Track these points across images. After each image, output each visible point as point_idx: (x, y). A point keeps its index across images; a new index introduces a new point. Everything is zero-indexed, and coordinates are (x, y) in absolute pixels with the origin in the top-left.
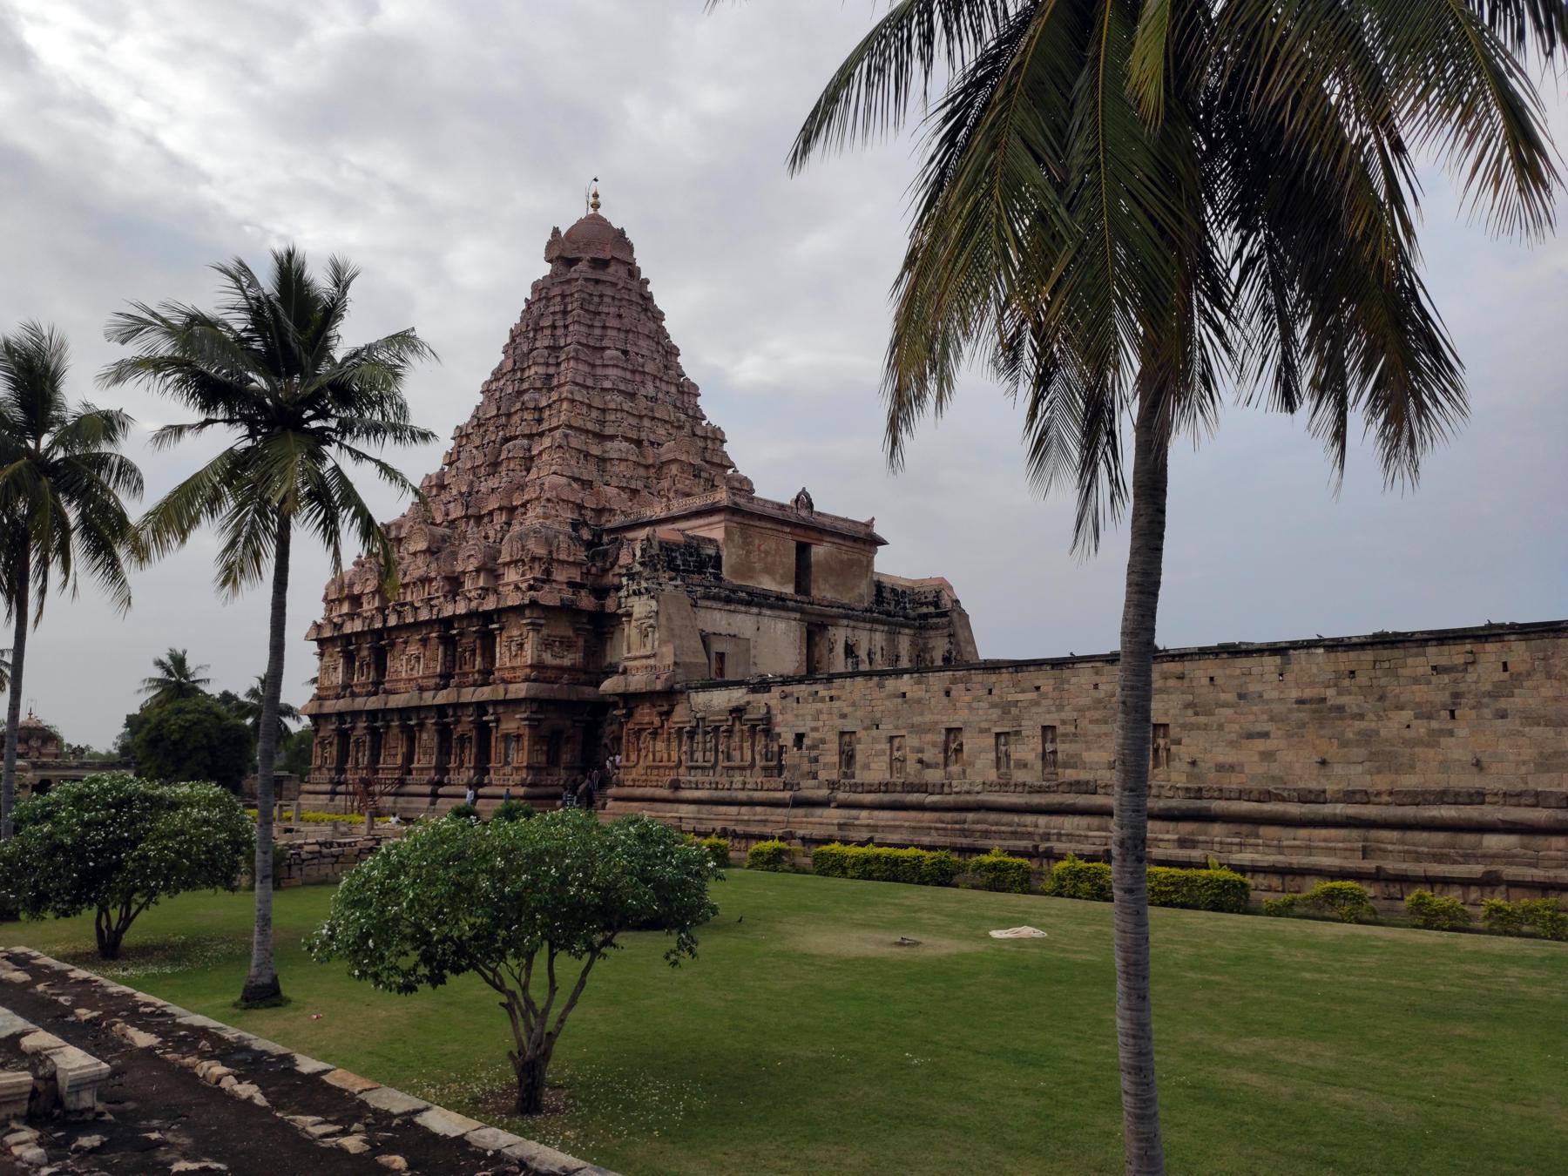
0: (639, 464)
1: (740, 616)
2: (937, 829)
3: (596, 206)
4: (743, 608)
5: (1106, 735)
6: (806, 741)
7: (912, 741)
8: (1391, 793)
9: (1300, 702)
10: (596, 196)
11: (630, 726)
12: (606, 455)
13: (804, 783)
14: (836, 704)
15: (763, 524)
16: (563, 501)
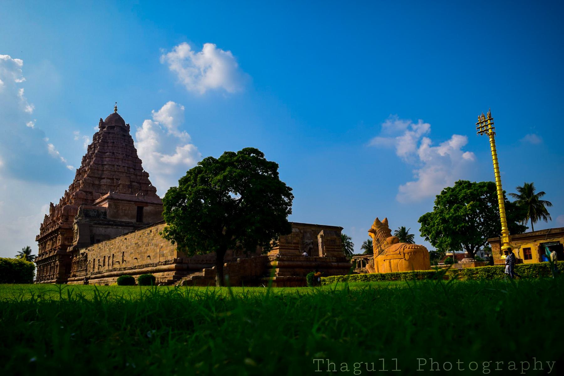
0: (111, 186)
1: (110, 229)
2: (97, 283)
3: (116, 110)
4: (110, 227)
5: (118, 255)
6: (90, 262)
7: (100, 261)
8: (141, 265)
9: (136, 244)
10: (116, 107)
11: (73, 261)
12: (101, 184)
13: (89, 273)
14: (94, 251)
15: (123, 202)
16: (79, 198)
